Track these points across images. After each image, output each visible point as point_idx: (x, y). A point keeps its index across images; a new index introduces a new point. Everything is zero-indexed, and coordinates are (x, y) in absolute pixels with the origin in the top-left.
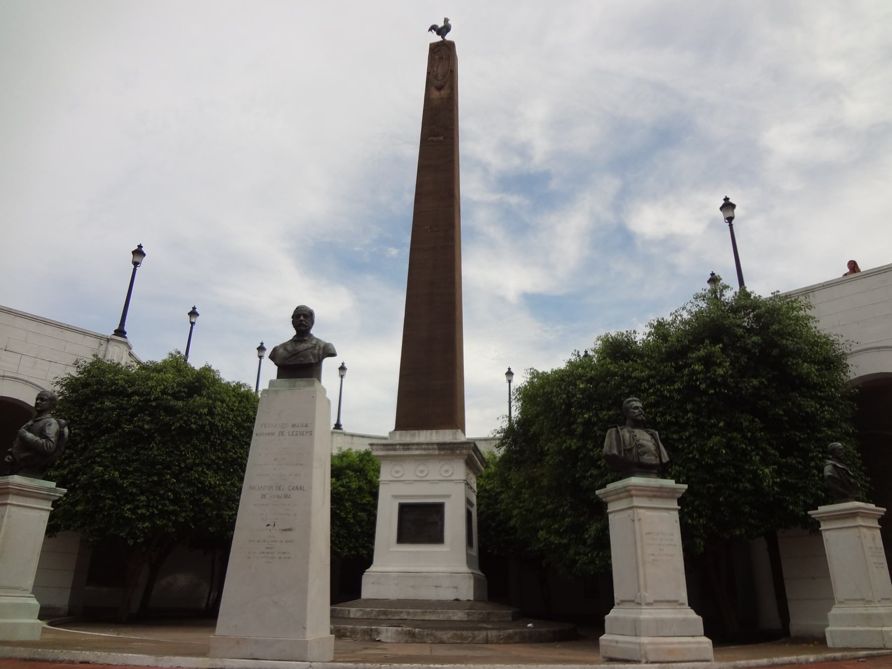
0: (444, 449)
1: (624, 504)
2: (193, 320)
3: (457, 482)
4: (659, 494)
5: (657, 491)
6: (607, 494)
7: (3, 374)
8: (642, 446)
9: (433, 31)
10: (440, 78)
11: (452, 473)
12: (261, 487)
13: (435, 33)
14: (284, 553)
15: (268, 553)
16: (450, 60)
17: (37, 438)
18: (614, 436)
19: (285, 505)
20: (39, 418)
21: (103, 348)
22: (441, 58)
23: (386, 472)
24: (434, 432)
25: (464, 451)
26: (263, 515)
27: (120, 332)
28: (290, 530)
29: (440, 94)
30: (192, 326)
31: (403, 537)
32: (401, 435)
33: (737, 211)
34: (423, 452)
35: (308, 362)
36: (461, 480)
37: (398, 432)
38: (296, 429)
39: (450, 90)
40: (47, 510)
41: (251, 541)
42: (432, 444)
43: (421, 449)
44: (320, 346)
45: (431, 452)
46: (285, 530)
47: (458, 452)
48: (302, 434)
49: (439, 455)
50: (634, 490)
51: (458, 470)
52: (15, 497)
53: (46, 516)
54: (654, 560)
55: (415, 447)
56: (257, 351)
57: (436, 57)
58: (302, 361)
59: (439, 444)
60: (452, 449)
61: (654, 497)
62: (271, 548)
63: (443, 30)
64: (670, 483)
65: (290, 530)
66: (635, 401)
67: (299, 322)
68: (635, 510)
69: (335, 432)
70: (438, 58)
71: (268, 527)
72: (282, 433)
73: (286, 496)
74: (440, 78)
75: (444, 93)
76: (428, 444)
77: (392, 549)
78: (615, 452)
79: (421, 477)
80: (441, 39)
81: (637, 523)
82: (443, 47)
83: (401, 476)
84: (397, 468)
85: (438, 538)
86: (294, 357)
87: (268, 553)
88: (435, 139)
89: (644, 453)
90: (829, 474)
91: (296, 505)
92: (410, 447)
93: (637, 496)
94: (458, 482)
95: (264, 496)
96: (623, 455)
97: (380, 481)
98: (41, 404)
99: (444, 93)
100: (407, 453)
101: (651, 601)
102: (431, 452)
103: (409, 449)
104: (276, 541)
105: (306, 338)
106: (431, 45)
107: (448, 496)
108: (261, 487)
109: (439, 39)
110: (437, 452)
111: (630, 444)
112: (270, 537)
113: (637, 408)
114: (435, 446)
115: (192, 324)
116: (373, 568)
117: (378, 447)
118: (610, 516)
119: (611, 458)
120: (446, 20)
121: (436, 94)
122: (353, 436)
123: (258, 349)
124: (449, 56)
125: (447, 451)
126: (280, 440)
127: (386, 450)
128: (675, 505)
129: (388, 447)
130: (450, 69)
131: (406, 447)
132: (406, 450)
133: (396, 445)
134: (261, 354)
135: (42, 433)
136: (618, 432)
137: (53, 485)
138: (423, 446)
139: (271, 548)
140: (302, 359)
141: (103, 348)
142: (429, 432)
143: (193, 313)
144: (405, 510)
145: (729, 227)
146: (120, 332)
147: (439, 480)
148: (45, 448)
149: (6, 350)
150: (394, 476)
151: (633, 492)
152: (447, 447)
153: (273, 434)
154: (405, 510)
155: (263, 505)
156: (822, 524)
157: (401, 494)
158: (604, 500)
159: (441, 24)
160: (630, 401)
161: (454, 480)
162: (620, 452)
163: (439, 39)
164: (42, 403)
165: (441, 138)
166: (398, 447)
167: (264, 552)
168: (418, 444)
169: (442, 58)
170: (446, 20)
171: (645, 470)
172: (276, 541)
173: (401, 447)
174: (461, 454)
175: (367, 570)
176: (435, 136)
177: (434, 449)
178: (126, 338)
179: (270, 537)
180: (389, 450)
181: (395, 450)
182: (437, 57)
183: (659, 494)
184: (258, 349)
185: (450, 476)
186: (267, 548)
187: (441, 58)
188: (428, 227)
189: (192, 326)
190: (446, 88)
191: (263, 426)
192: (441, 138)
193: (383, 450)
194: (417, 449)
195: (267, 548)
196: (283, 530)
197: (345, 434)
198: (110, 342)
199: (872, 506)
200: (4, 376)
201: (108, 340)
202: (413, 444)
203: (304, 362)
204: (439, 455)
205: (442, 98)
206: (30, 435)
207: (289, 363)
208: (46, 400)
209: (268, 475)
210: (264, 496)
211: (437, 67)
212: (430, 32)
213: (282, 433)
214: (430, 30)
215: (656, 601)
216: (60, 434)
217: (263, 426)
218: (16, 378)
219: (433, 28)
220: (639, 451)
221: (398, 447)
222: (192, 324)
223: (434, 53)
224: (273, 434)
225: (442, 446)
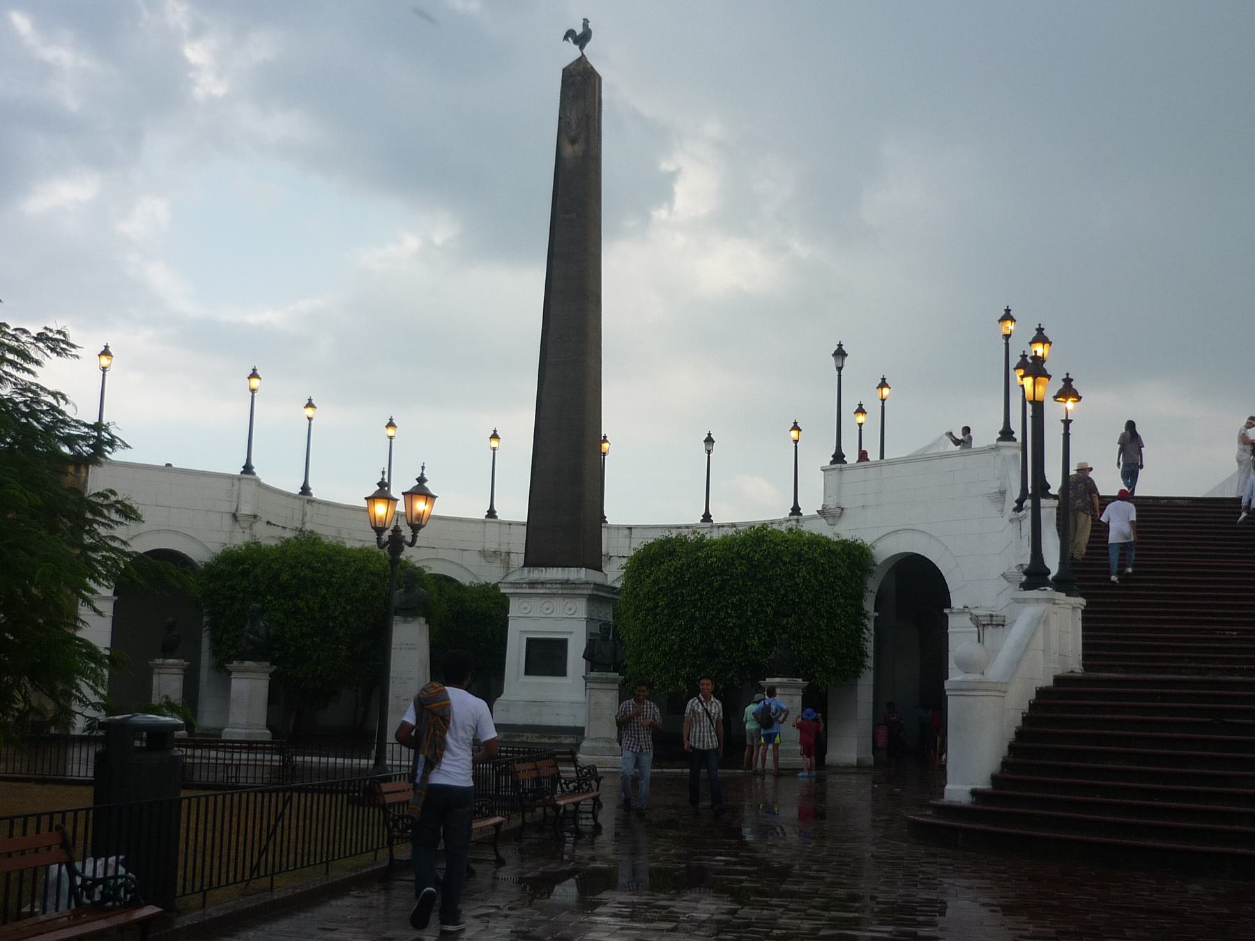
3: (579, 619)
7: (157, 529)
9: (570, 39)
10: (574, 126)
21: (236, 488)
27: (248, 469)
31: (529, 670)
32: (529, 572)
33: (847, 359)
37: (526, 569)
43: (545, 588)
45: (554, 591)
51: (580, 608)
55: (539, 586)
69: (489, 522)
73: (405, 683)
79: (547, 614)
84: (525, 605)
85: (562, 672)
92: (536, 586)
99: (578, 148)
101: (593, 737)
103: (534, 588)
106: (563, 70)
107: (571, 633)
116: (502, 698)
117: (506, 585)
120: (586, 22)
122: (510, 524)
127: (514, 588)
128: (616, 686)
129: (516, 585)
131: (532, 586)
133: (522, 583)
138: (548, 586)
141: (236, 488)
144: (534, 645)
146: (248, 469)
149: (156, 506)
168: (542, 583)
170: (586, 22)
173: (527, 586)
174: (581, 595)
175: (498, 699)
177: (557, 588)
178: (254, 474)
180: (517, 588)
181: (521, 588)
185: (573, 614)
193: (510, 588)
194: (541, 588)
197: (501, 523)
199: (800, 680)
200: (159, 530)
201: (239, 479)
204: (562, 594)
213: (401, 648)
214: (566, 38)
215: (596, 738)
218: (169, 530)
219: (570, 34)
221: (524, 585)
225: (565, 583)
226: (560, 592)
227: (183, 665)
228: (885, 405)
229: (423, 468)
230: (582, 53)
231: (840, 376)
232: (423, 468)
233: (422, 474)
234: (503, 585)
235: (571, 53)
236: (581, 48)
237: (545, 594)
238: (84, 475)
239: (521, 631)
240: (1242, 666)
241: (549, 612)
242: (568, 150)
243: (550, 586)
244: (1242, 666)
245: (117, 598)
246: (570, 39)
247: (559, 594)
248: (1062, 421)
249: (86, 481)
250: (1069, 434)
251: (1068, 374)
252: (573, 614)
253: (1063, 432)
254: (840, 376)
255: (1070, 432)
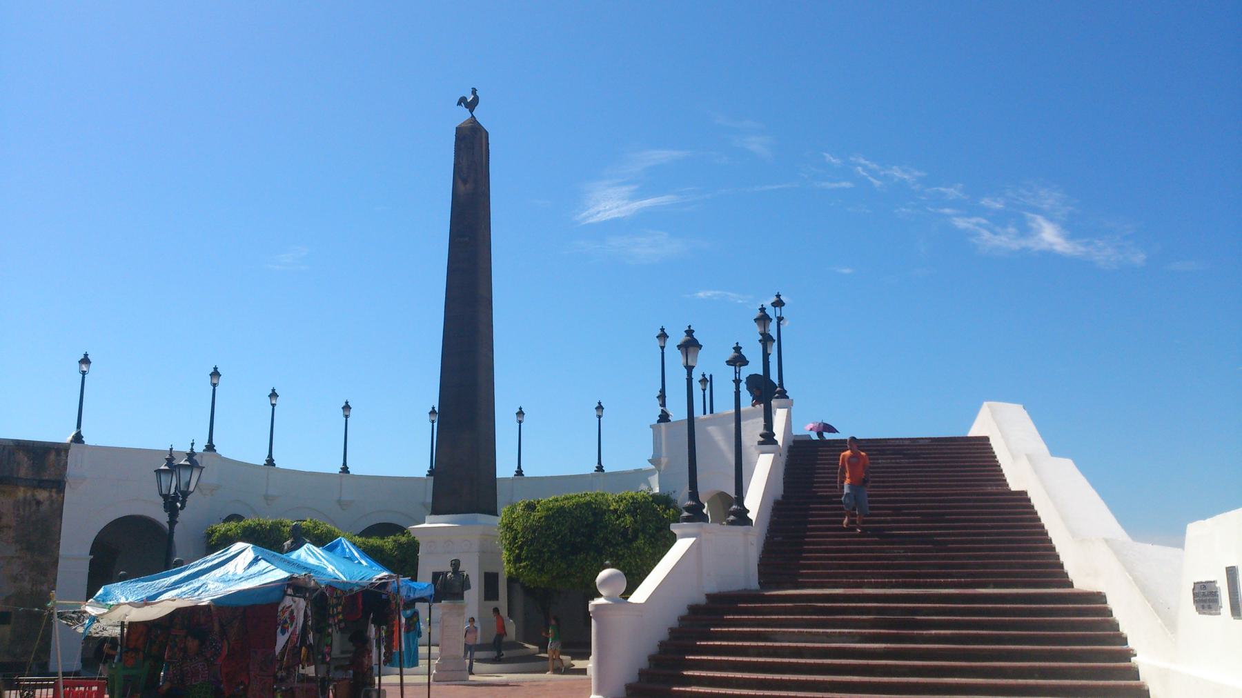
2: (274, 402)
9: (462, 104)
30: (273, 407)
56: (342, 410)
115: (273, 405)
120: (474, 91)
121: (462, 188)
123: (343, 408)
143: (274, 395)
170: (474, 91)
184: (343, 408)
189: (273, 407)
214: (459, 104)
219: (462, 101)
222: (273, 405)
229: (193, 444)
230: (472, 115)
231: (663, 353)
232: (193, 444)
233: (192, 449)
235: (463, 115)
236: (471, 111)
238: (64, 458)
240: (890, 580)
242: (462, 188)
244: (890, 580)
245: (92, 557)
246: (462, 104)
248: (734, 381)
249: (66, 463)
250: (740, 392)
251: (737, 343)
253: (735, 390)
254: (663, 353)
255: (740, 389)
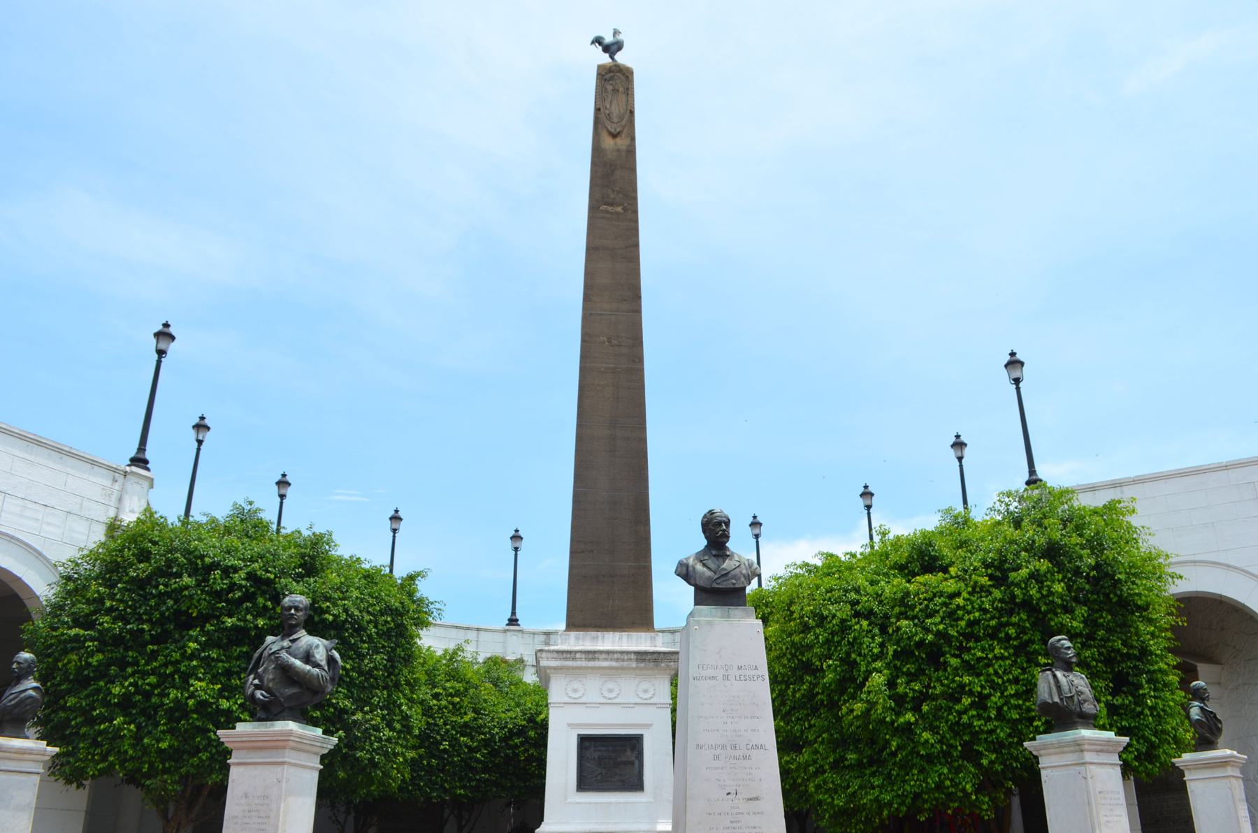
0: (644, 660)
1: (1070, 758)
4: (1106, 748)
5: (1105, 745)
6: (1045, 747)
8: (1082, 693)
9: (597, 45)
11: (654, 694)
12: (712, 745)
13: (600, 48)
14: (754, 828)
15: (734, 828)
16: (630, 95)
17: (308, 667)
18: (1051, 677)
19: (746, 768)
20: (295, 636)
22: (616, 91)
23: (557, 692)
24: (624, 634)
25: (672, 663)
26: (720, 780)
28: (757, 799)
29: (616, 144)
31: (585, 782)
32: (577, 638)
34: (614, 664)
35: (741, 585)
36: (665, 704)
37: (573, 634)
38: (741, 672)
39: (629, 139)
40: (316, 769)
41: (710, 814)
42: (628, 653)
44: (744, 564)
46: (751, 799)
47: (663, 665)
48: (752, 678)
49: (637, 668)
50: (1089, 744)
52: (294, 753)
53: (316, 775)
54: (1108, 822)
55: (603, 656)
57: (607, 87)
58: (734, 584)
59: (638, 653)
60: (656, 660)
61: (1101, 751)
62: (736, 822)
63: (611, 48)
64: (1110, 735)
65: (757, 799)
66: (1065, 639)
67: (720, 532)
68: (1087, 766)
70: (613, 90)
71: (730, 795)
72: (726, 677)
73: (745, 757)
74: (615, 120)
75: (621, 142)
76: (622, 653)
77: (569, 800)
78: (1056, 699)
80: (610, 60)
81: (1090, 780)
82: (618, 74)
83: (580, 698)
84: (576, 685)
86: (722, 579)
87: (734, 828)
88: (610, 209)
89: (1085, 701)
90: (1197, 717)
91: (759, 768)
93: (1088, 751)
94: (661, 706)
95: (717, 757)
96: (1065, 703)
97: (550, 703)
98: (296, 615)
99: (621, 142)
100: (591, 664)
102: (625, 664)
103: (594, 659)
104: (742, 814)
105: (728, 553)
106: (599, 67)
107: (648, 726)
108: (712, 745)
109: (605, 59)
110: (634, 664)
111: (1070, 690)
112: (733, 808)
113: (1069, 648)
114: (633, 656)
116: (543, 825)
117: (549, 655)
118: (1043, 773)
119: (1047, 708)
121: (608, 143)
124: (628, 89)
125: (647, 663)
126: (725, 686)
129: (565, 655)
130: (629, 108)
131: (590, 656)
132: (589, 660)
133: (576, 652)
134: (282, 492)
135: (308, 658)
136: (1055, 676)
137: (319, 731)
138: (615, 656)
139: (736, 822)
140: (734, 581)
142: (617, 634)
144: (585, 742)
145: (1015, 390)
147: (635, 704)
148: (322, 682)
150: (570, 697)
151: (1086, 747)
152: (649, 657)
153: (715, 678)
154: (585, 742)
155: (717, 768)
156: (1186, 773)
157: (609, 722)
158: (1034, 753)
159: (609, 39)
160: (1060, 640)
161: (656, 704)
162: (1061, 699)
163: (605, 59)
164: (298, 614)
165: (619, 209)
166: (578, 655)
167: (729, 828)
168: (608, 652)
169: (618, 91)
170: (616, 33)
171: (1089, 720)
172: (742, 814)
173: (584, 656)
176: (611, 204)
179: (733, 808)
180: (566, 659)
181: (574, 659)
182: (610, 88)
183: (1106, 748)
186: (732, 822)
187: (616, 91)
188: (606, 339)
190: (623, 136)
191: (701, 667)
192: (619, 209)
193: (556, 659)
194: (606, 659)
195: (732, 822)
196: (751, 799)
198: (128, 477)
202: (601, 652)
203: (737, 586)
204: (637, 668)
205: (619, 150)
206: (298, 663)
207: (718, 586)
208: (301, 610)
209: (718, 730)
210: (717, 757)
211: (611, 102)
212: (593, 46)
213: (726, 677)
214: (593, 43)
216: (331, 660)
217: (701, 667)
219: (598, 41)
220: (1080, 699)
223: (605, 80)
224: (715, 678)
225: (641, 656)
226: (634, 666)
227: (44, 753)
228: (963, 464)
234: (544, 655)
236: (612, 57)
237: (610, 668)
239: (569, 725)
241: (613, 695)
243: (619, 656)
247: (633, 669)
252: (651, 697)
